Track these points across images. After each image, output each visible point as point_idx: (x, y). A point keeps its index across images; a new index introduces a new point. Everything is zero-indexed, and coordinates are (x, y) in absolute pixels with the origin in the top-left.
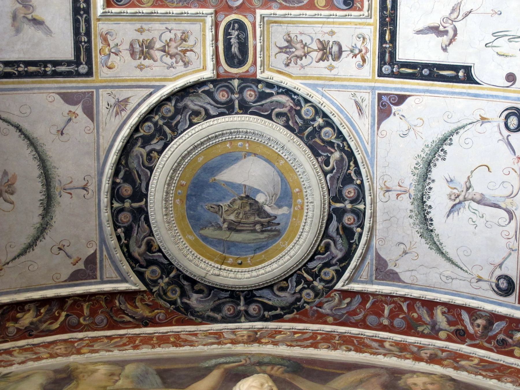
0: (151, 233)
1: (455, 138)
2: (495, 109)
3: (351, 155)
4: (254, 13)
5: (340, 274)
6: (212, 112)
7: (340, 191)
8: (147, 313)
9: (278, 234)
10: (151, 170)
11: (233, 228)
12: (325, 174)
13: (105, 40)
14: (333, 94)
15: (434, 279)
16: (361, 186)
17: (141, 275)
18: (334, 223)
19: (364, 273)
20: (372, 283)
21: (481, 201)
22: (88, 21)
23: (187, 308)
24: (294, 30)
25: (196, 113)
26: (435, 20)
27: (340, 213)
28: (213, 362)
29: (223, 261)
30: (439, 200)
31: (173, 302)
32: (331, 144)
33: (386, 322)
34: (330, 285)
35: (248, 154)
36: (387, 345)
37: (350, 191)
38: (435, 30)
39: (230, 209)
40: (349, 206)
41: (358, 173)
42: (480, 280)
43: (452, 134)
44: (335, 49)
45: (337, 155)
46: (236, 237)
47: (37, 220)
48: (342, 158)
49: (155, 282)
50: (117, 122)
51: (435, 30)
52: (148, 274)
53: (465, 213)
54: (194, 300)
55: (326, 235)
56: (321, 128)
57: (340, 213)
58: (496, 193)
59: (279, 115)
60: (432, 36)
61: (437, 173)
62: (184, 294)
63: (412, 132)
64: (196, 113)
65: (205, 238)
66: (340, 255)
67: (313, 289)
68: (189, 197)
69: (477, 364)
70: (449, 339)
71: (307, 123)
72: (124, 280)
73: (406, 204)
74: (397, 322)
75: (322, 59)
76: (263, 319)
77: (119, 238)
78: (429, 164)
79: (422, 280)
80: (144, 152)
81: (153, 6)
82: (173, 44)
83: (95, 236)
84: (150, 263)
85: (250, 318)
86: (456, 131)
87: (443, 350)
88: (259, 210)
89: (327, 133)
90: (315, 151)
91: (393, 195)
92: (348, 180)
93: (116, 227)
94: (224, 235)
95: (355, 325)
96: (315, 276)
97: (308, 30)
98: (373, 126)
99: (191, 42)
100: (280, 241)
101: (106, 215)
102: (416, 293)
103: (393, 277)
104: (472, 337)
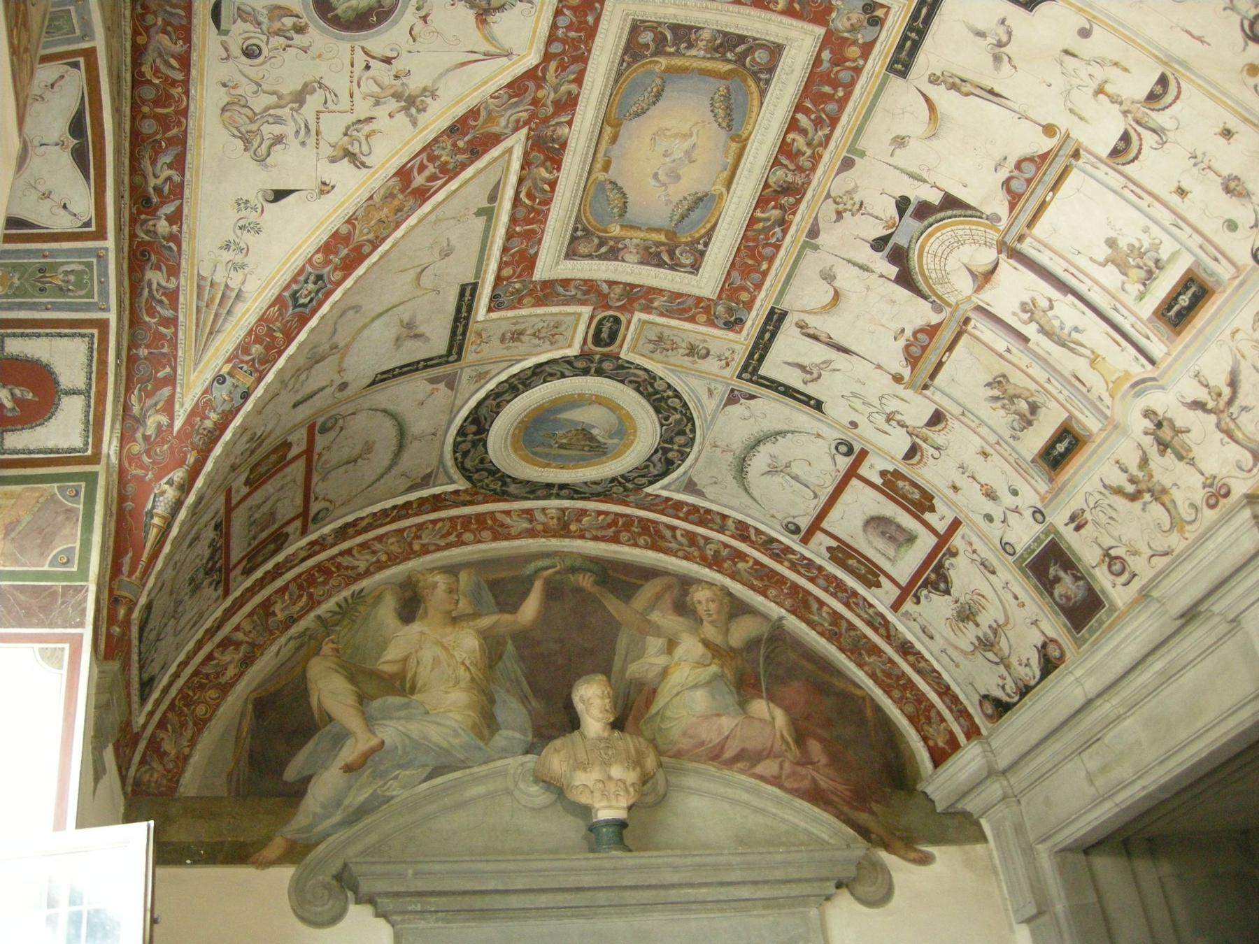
0: (486, 452)
1: (789, 436)
2: (833, 435)
3: (691, 419)
4: (632, 313)
5: (651, 483)
6: (567, 373)
7: (672, 438)
8: (468, 498)
9: (605, 453)
10: (498, 413)
11: (562, 446)
12: (662, 425)
13: (479, 335)
14: (690, 380)
15: (735, 502)
16: (693, 440)
17: (469, 479)
18: (659, 454)
19: (673, 487)
20: (678, 492)
21: (796, 478)
22: (466, 326)
23: (504, 493)
24: (666, 332)
25: (551, 375)
26: (804, 361)
27: (665, 451)
28: (532, 567)
29: (548, 465)
30: (759, 462)
31: (494, 490)
32: (675, 409)
33: (681, 515)
34: (639, 488)
35: (594, 402)
36: (678, 533)
37: (680, 440)
38: (803, 368)
39: (565, 436)
40: (676, 447)
41: (693, 431)
42: (773, 516)
43: (788, 432)
44: (704, 352)
45: (678, 416)
46: (563, 452)
47: (387, 462)
48: (681, 420)
49: (481, 481)
50: (473, 388)
51: (803, 368)
52: (476, 476)
53: (778, 479)
54: (512, 488)
55: (649, 460)
56: (669, 397)
57: (665, 451)
58: (812, 480)
59: (630, 382)
60: (798, 372)
61: (765, 451)
62: (504, 484)
63: (752, 420)
64: (551, 375)
65: (535, 454)
66: (656, 473)
67: (624, 487)
68: (527, 428)
69: (751, 568)
70: (733, 537)
71: (657, 392)
72: (453, 482)
73: (729, 457)
74: (691, 517)
75: (688, 355)
76: (572, 498)
77: (456, 459)
78: (759, 442)
79: (724, 500)
80: (494, 403)
81: (533, 306)
82: (544, 331)
83: (435, 462)
84: (478, 470)
85: (558, 496)
86: (793, 432)
87: (726, 546)
88: (592, 438)
89: (675, 402)
90: (657, 411)
91: (719, 450)
92: (683, 433)
93: (455, 452)
94: (556, 451)
95: (654, 511)
96: (628, 480)
97: (684, 335)
98: (718, 406)
99: (561, 329)
100: (604, 458)
101: (448, 447)
102: (715, 508)
103: (700, 494)
104: (752, 542)
